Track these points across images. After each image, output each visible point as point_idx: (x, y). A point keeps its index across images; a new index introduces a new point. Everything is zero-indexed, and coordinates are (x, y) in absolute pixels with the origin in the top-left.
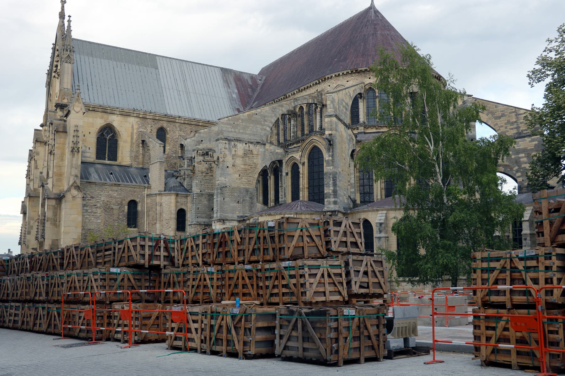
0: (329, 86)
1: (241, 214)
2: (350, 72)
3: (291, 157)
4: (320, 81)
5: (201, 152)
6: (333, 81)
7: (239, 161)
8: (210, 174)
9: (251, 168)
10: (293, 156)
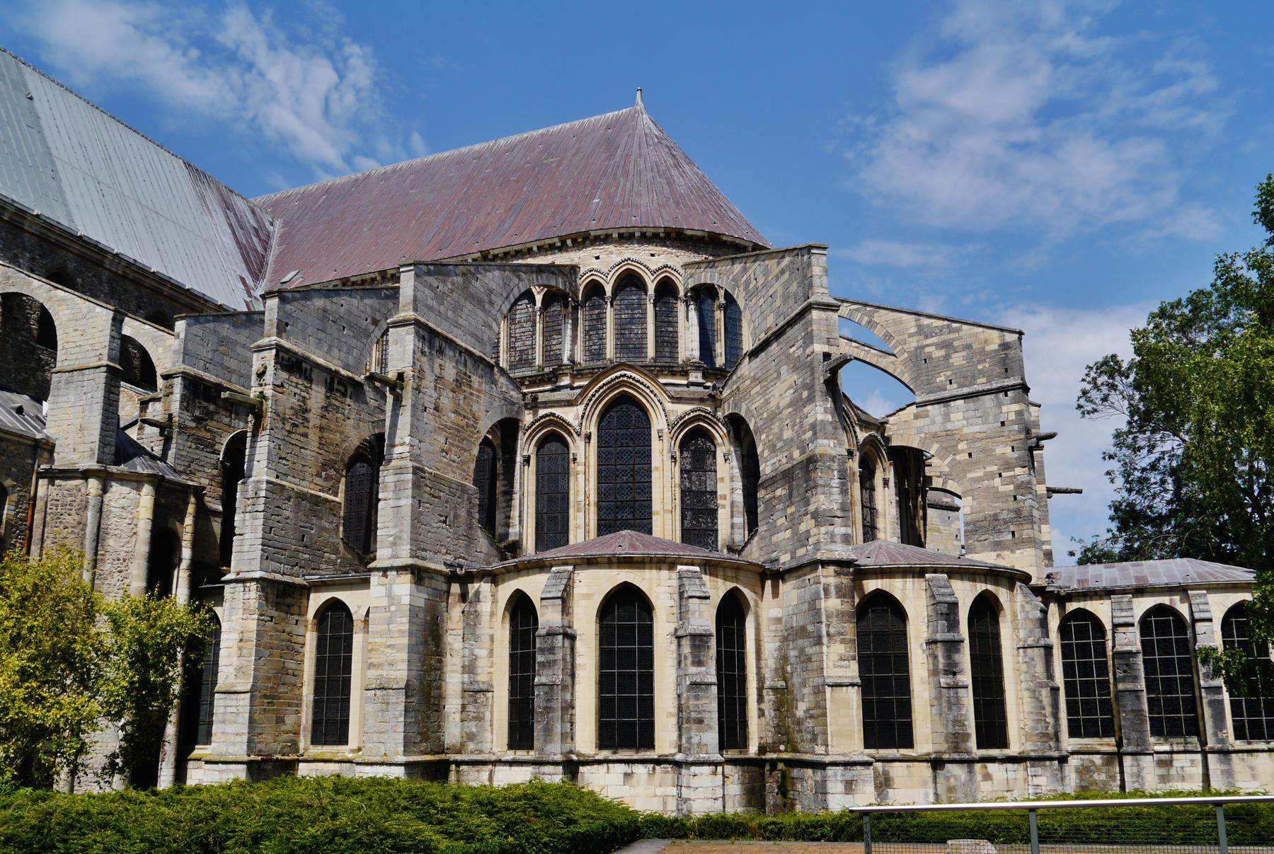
0: (597, 258)
1: (450, 558)
2: (662, 235)
3: (546, 416)
4: (569, 242)
5: (286, 356)
6: (611, 247)
7: (446, 401)
8: (301, 430)
9: (467, 425)
10: (553, 415)
